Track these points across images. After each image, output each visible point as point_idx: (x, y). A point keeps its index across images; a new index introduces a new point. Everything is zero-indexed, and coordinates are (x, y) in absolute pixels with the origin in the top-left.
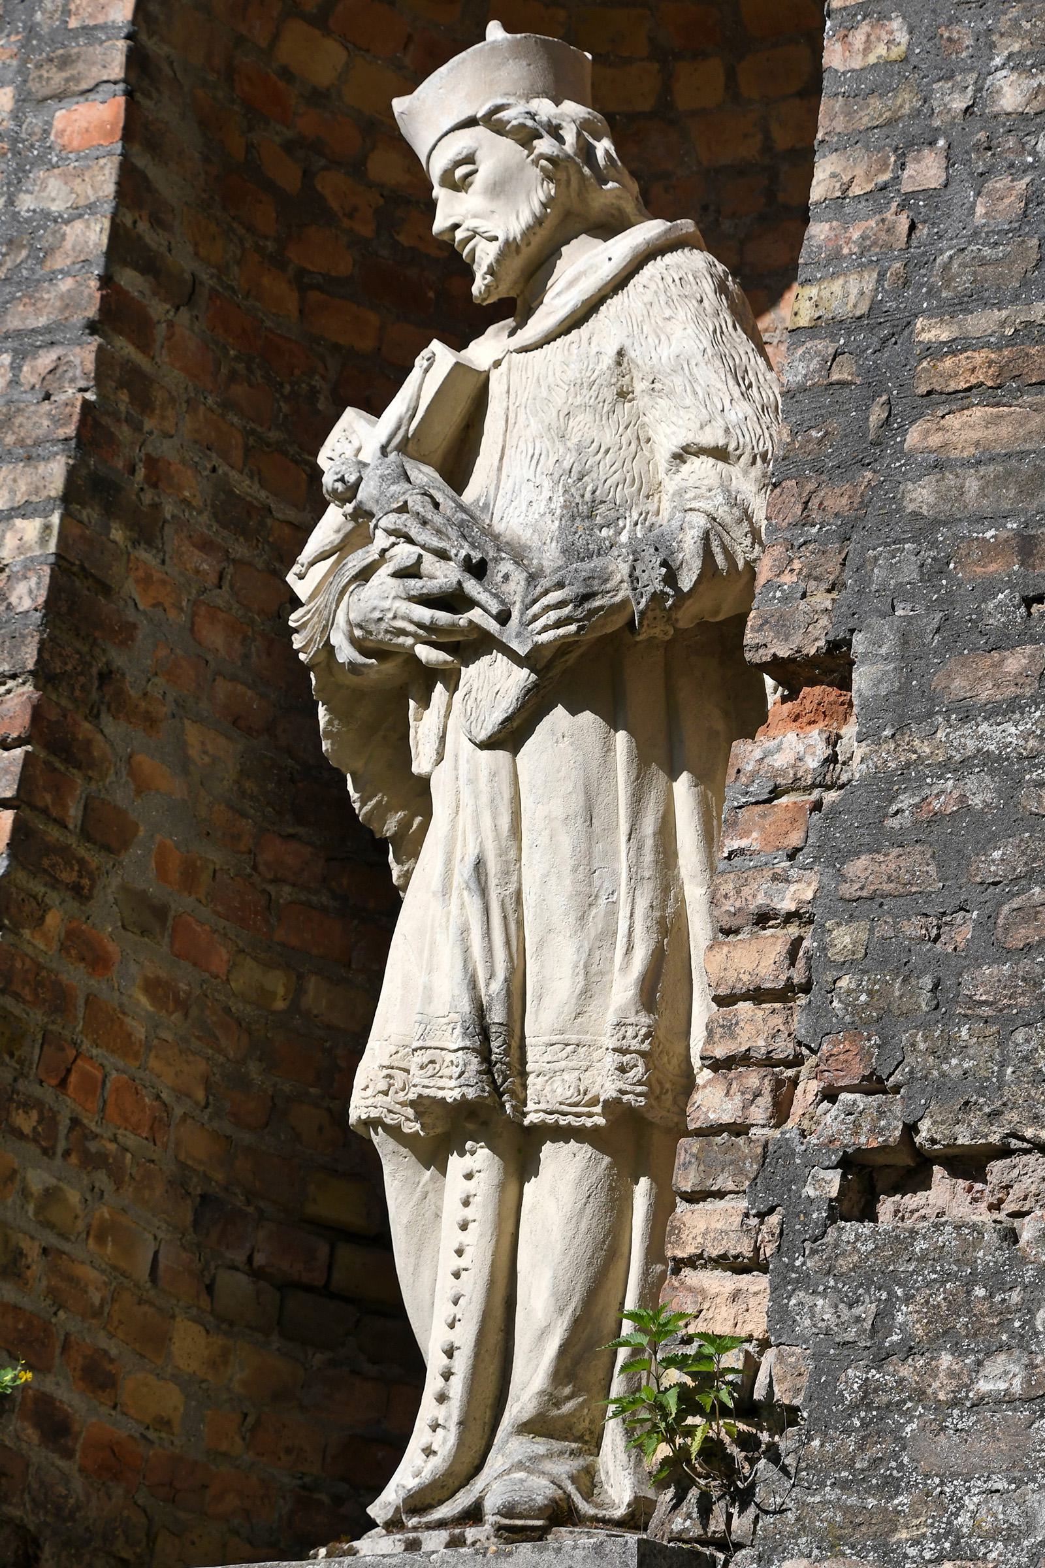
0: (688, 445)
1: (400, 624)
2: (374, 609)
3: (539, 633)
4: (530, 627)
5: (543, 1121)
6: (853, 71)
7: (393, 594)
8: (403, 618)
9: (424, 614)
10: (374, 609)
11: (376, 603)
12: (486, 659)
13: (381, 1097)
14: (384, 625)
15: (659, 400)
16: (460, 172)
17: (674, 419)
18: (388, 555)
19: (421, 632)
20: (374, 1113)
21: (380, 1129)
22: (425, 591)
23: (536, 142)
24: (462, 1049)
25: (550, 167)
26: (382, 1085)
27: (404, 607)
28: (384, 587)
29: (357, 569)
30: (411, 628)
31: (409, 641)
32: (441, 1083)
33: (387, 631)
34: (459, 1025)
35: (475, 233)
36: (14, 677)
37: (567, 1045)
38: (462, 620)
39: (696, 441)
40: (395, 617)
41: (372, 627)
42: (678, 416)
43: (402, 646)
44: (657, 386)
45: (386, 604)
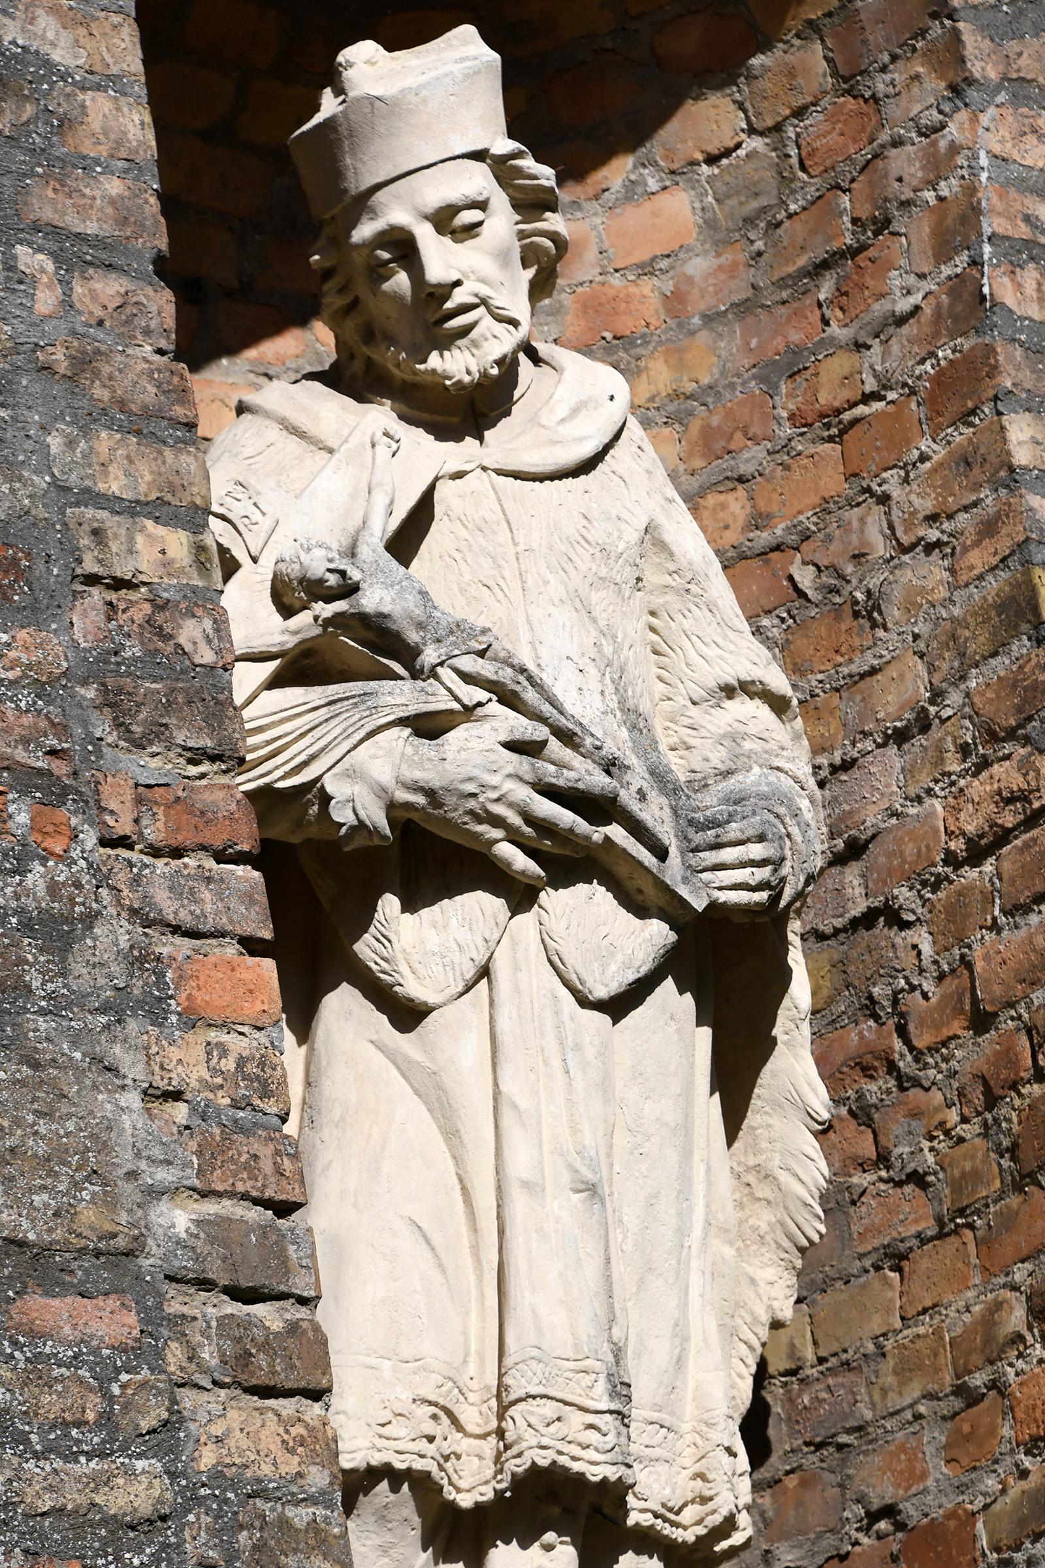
0: (753, 682)
1: (499, 809)
2: (470, 779)
3: (720, 889)
4: (706, 876)
5: (652, 1526)
6: (1031, 320)
7: (510, 769)
8: (511, 805)
9: (547, 808)
10: (470, 779)
11: (476, 772)
12: (582, 889)
13: (424, 1445)
14: (471, 804)
15: (693, 608)
16: (468, 217)
17: (718, 640)
18: (480, 711)
19: (528, 830)
20: (419, 1465)
21: (405, 1487)
22: (581, 786)
23: (548, 214)
24: (611, 1412)
25: (554, 251)
26: (429, 1427)
27: (524, 793)
28: (492, 756)
29: (411, 710)
30: (515, 820)
31: (497, 833)
32: (576, 1451)
33: (471, 812)
34: (602, 1378)
35: (484, 302)
36: (214, 759)
37: (662, 1427)
38: (597, 834)
39: (765, 680)
40: (498, 800)
41: (450, 800)
42: (725, 637)
43: (477, 836)
44: (692, 587)
45: (494, 780)
